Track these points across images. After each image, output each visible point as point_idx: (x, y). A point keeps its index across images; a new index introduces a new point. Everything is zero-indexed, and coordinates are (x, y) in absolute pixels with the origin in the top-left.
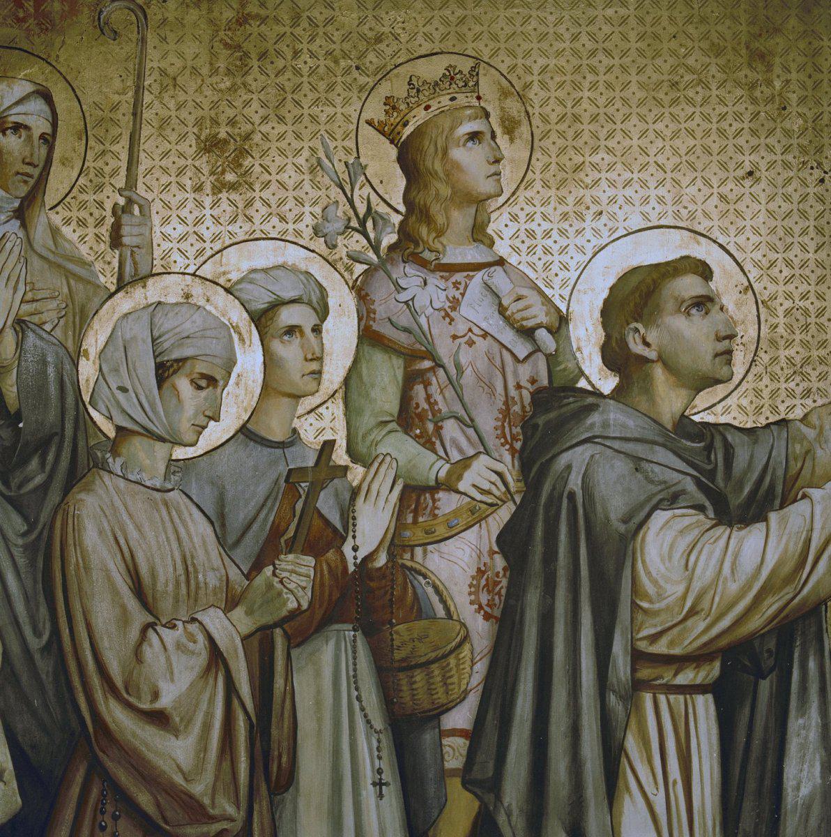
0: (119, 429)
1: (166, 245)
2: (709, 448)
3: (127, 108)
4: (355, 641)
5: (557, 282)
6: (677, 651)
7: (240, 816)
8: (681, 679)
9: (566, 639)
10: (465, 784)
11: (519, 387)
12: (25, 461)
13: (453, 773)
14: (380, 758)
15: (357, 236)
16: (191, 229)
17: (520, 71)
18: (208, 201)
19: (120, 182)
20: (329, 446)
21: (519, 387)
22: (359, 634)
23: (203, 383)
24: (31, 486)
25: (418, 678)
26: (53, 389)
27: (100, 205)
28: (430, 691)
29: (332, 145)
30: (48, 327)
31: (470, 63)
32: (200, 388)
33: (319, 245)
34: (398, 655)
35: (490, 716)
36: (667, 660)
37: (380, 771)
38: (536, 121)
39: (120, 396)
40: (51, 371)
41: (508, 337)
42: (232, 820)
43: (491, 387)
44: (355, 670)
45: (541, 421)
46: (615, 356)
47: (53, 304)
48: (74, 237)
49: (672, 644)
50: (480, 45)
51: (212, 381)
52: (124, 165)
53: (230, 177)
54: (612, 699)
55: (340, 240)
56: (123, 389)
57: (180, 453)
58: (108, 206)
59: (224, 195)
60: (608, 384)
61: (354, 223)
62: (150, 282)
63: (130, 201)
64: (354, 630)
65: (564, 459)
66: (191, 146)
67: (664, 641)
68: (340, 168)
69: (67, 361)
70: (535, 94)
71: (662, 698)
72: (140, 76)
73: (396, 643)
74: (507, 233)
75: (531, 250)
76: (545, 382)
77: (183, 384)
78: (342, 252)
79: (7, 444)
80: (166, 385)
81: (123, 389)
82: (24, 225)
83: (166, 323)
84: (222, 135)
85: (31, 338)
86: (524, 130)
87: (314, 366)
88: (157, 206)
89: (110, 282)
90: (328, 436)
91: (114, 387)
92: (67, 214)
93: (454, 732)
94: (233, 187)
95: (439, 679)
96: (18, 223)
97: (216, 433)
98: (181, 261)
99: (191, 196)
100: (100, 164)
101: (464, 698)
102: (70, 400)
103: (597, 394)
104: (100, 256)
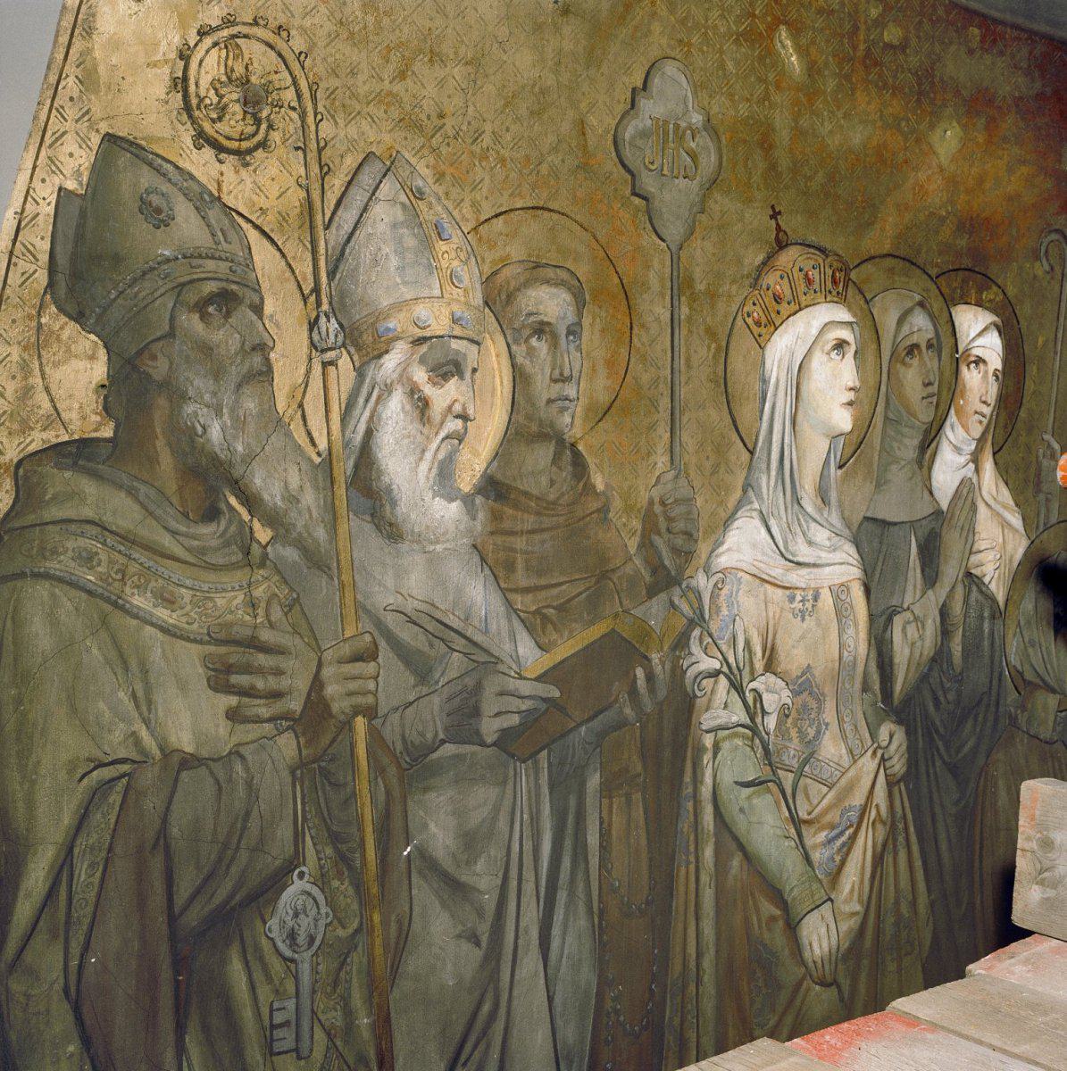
26: (986, 643)
39: (1030, 650)
40: (986, 625)
96: (972, 466)
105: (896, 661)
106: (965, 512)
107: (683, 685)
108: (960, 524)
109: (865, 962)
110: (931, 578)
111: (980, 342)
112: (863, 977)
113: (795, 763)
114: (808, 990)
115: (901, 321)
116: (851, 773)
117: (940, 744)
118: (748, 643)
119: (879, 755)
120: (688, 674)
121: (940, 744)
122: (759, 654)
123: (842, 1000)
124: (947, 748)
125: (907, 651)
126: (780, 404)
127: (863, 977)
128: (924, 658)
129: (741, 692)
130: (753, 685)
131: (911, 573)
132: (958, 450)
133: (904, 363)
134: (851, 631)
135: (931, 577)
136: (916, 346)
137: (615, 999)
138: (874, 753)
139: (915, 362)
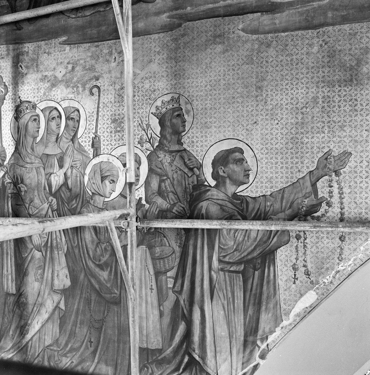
0: (93, 193)
1: (104, 147)
2: (242, 202)
3: (95, 113)
5: (200, 155)
11: (189, 184)
12: (72, 200)
15: (149, 143)
16: (109, 143)
17: (191, 97)
18: (113, 135)
19: (94, 131)
20: (141, 199)
21: (189, 184)
23: (112, 182)
24: (73, 207)
26: (79, 182)
27: (89, 137)
29: (143, 119)
30: (78, 168)
31: (178, 95)
32: (111, 183)
33: (139, 146)
38: (195, 110)
39: (93, 185)
40: (78, 178)
41: (186, 170)
43: (182, 184)
45: (195, 194)
46: (215, 176)
47: (78, 162)
48: (84, 145)
50: (180, 90)
51: (113, 181)
52: (95, 127)
53: (118, 129)
55: (144, 145)
56: (94, 183)
57: (106, 200)
58: (91, 137)
59: (117, 134)
60: (213, 183)
61: (148, 140)
62: (100, 156)
63: (96, 136)
65: (201, 204)
66: (109, 122)
68: (145, 126)
69: (82, 176)
70: (195, 103)
72: (99, 104)
74: (187, 142)
75: (193, 146)
76: (196, 183)
77: (107, 182)
78: (144, 148)
79: (69, 196)
80: (103, 182)
81: (94, 183)
82: (73, 143)
83: (104, 166)
84: (117, 118)
85: (74, 171)
86: (192, 113)
87: (137, 178)
88: (102, 137)
89: (91, 156)
90: (141, 196)
91: (92, 182)
92: (82, 140)
94: (119, 131)
96: (71, 142)
97: (114, 195)
98: (107, 151)
99: (109, 134)
100: (89, 127)
102: (82, 186)
103: (210, 186)
104: (89, 150)
105: (52, 184)
106: (70, 152)
108: (69, 154)
109: (49, 249)
110: (61, 167)
111: (72, 114)
112: (48, 252)
113: (29, 203)
115: (50, 113)
116: (41, 207)
117: (66, 204)
118: (17, 178)
119: (49, 204)
121: (66, 204)
122: (20, 180)
123: (43, 255)
124: (68, 206)
126: (22, 132)
127: (48, 252)
129: (16, 188)
131: (55, 165)
132: (67, 139)
133: (51, 121)
134: (41, 177)
135: (61, 167)
136: (55, 117)
138: (48, 203)
139: (54, 121)
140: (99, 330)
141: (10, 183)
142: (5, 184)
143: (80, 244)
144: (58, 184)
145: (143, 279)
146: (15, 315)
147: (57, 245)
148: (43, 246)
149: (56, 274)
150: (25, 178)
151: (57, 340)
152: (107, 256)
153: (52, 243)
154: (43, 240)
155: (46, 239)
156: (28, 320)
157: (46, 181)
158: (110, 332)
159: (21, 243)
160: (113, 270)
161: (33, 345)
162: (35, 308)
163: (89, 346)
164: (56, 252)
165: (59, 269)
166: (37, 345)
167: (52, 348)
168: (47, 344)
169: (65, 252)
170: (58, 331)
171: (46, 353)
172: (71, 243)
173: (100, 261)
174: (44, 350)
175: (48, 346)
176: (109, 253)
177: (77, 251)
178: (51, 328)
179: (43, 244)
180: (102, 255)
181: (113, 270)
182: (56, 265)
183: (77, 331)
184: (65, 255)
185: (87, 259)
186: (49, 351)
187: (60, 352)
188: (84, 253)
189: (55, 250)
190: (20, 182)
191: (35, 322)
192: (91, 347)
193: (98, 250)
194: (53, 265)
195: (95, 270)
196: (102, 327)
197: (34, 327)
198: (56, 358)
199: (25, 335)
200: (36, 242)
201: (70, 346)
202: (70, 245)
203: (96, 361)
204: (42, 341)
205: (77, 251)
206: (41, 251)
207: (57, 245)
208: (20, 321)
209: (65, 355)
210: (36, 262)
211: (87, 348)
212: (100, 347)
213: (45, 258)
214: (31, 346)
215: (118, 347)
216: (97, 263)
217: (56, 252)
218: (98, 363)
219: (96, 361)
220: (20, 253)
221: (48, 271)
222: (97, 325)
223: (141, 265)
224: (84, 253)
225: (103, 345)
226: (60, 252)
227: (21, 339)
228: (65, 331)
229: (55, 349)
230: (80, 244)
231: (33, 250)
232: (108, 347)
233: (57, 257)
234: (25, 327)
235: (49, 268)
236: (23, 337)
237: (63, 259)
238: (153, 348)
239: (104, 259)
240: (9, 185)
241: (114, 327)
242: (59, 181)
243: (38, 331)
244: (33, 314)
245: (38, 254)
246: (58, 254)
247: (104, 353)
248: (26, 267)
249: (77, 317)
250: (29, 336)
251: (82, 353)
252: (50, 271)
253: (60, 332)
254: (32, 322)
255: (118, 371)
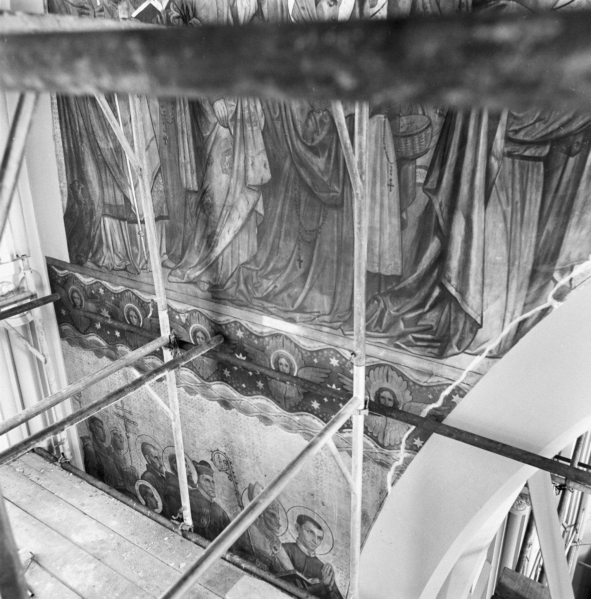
4: (385, 123)
6: (528, 139)
7: (340, 191)
8: (527, 153)
9: (474, 128)
10: (425, 190)
13: (420, 184)
14: (391, 174)
22: (387, 119)
25: (408, 141)
28: (413, 148)
34: (401, 130)
35: (437, 161)
36: (522, 143)
37: (391, 180)
42: (337, 193)
44: (384, 135)
49: (525, 135)
54: (493, 160)
56: (303, 8)
64: (385, 118)
67: (522, 133)
71: (517, 161)
73: (401, 125)
80: (318, 5)
81: (303, 8)
91: (300, 7)
93: (420, 167)
95: (417, 142)
101: (426, 153)
105: (239, 14)
107: (170, 22)
109: (239, 124)
114: (219, 127)
118: (187, 7)
120: (171, 17)
122: (191, 11)
123: (231, 134)
125: (244, 11)
128: (251, 12)
130: (190, 21)
137: (164, 112)
140: (312, 244)
141: (178, 17)
142: (171, 19)
143: (284, 113)
144: (248, 13)
145: (378, 169)
146: (199, 221)
147: (250, 117)
148: (231, 120)
149: (250, 163)
150: (198, 7)
151: (255, 256)
152: (324, 133)
153: (242, 115)
154: (229, 109)
155: (234, 108)
156: (217, 228)
157: (229, 10)
158: (326, 247)
159: (200, 115)
160: (333, 154)
161: (225, 261)
162: (224, 212)
163: (297, 265)
164: (249, 129)
165: (254, 155)
166: (230, 262)
167: (248, 266)
168: (242, 260)
169: (262, 128)
170: (256, 244)
171: (241, 272)
172: (270, 114)
173: (313, 140)
174: (238, 269)
175: (243, 264)
176: (326, 128)
177: (278, 126)
178: (247, 240)
179: (230, 117)
180: (316, 131)
181: (333, 154)
182: (249, 147)
183: (281, 246)
184: (263, 133)
185: (294, 138)
186: (245, 270)
187: (260, 273)
188: (289, 129)
189: (247, 125)
190: (191, 14)
191: (225, 230)
192: (300, 268)
193: (310, 123)
194: (246, 148)
195: (305, 155)
196: (315, 241)
197: (224, 238)
198: (255, 280)
199: (213, 247)
200: (220, 112)
201: (271, 265)
202: (268, 116)
203: (307, 287)
204: (235, 256)
205: (278, 126)
206: (228, 127)
207: (250, 117)
208: (206, 229)
209: (266, 277)
210: (222, 144)
211: (294, 268)
212: (312, 269)
213: (234, 137)
214: (222, 262)
215: (338, 269)
216: (309, 144)
217: (249, 129)
218: (310, 289)
219: (307, 287)
220: (199, 130)
221: (239, 157)
222: (308, 238)
223: (376, 147)
224: (289, 129)
225: (317, 265)
226: (255, 128)
227: (209, 253)
228: (265, 244)
229: (253, 267)
230: (284, 113)
231: (217, 126)
232: (323, 269)
233: (251, 137)
234: (213, 237)
235: (239, 153)
236: (212, 251)
237: (260, 139)
238: (387, 274)
239: (319, 138)
240: (177, 20)
241: (332, 241)
242: (248, 8)
243: (230, 243)
244: (222, 219)
245: (224, 132)
246: (252, 131)
247: (318, 276)
248: (208, 152)
249: (280, 225)
250: (218, 250)
251: (289, 275)
252: (242, 157)
253: (258, 246)
254: (221, 231)
255: (337, 303)
